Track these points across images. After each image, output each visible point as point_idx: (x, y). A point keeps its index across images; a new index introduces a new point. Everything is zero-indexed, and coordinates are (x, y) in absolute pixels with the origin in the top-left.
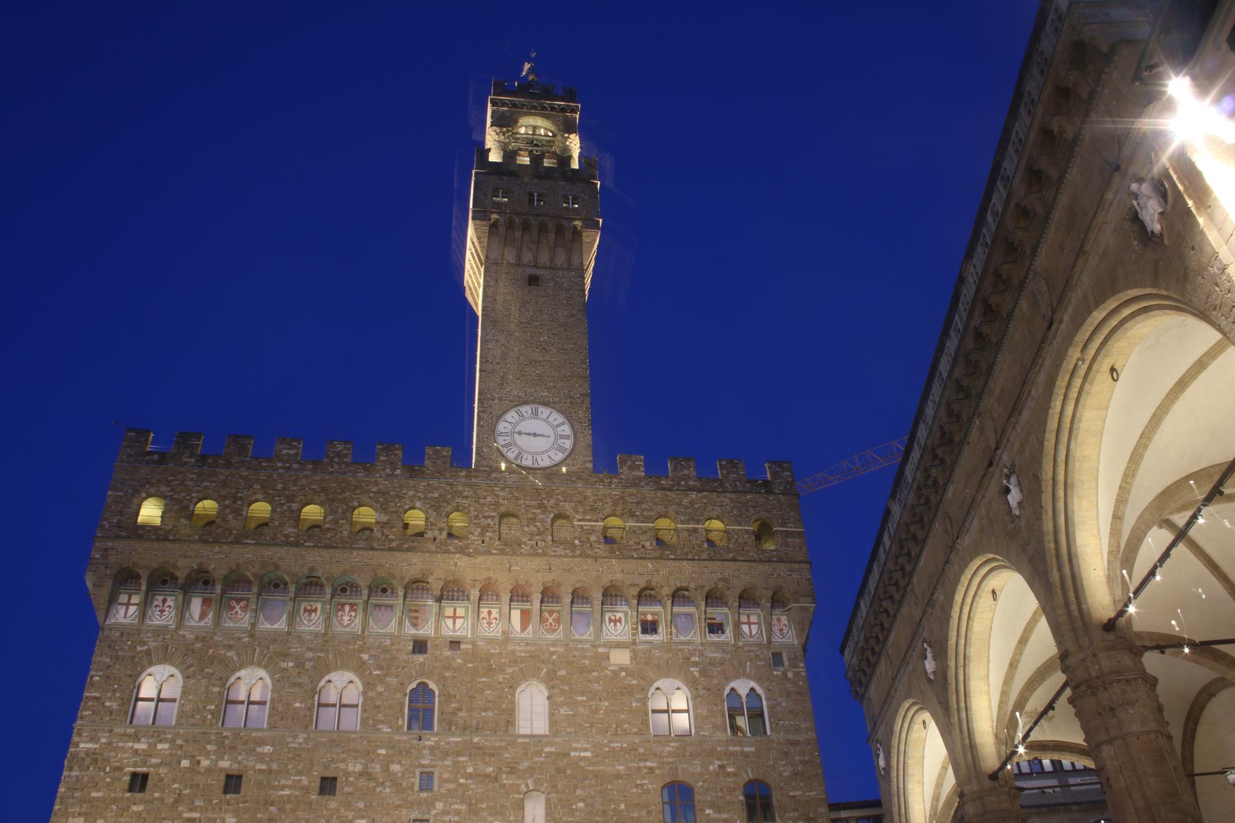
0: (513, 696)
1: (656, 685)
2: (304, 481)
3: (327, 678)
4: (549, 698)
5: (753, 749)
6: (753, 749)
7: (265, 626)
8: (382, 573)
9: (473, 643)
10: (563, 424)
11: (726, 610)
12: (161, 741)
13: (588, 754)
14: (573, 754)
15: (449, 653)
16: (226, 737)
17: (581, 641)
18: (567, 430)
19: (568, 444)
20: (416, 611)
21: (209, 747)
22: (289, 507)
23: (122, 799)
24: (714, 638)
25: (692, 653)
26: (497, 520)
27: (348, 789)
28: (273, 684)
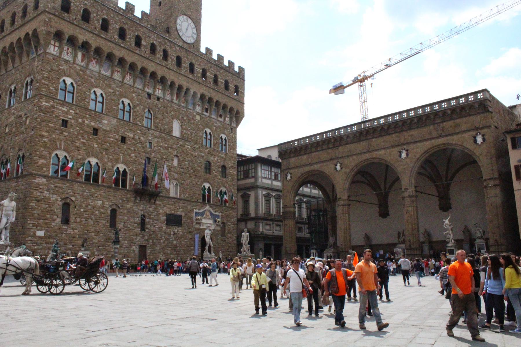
4: (181, 126)
8: (144, 65)
15: (157, 102)
16: (92, 114)
17: (189, 109)
18: (195, 31)
19: (195, 37)
20: (148, 83)
21: (87, 116)
23: (60, 129)
24: (220, 119)
25: (215, 122)
27: (130, 143)
28: (107, 98)
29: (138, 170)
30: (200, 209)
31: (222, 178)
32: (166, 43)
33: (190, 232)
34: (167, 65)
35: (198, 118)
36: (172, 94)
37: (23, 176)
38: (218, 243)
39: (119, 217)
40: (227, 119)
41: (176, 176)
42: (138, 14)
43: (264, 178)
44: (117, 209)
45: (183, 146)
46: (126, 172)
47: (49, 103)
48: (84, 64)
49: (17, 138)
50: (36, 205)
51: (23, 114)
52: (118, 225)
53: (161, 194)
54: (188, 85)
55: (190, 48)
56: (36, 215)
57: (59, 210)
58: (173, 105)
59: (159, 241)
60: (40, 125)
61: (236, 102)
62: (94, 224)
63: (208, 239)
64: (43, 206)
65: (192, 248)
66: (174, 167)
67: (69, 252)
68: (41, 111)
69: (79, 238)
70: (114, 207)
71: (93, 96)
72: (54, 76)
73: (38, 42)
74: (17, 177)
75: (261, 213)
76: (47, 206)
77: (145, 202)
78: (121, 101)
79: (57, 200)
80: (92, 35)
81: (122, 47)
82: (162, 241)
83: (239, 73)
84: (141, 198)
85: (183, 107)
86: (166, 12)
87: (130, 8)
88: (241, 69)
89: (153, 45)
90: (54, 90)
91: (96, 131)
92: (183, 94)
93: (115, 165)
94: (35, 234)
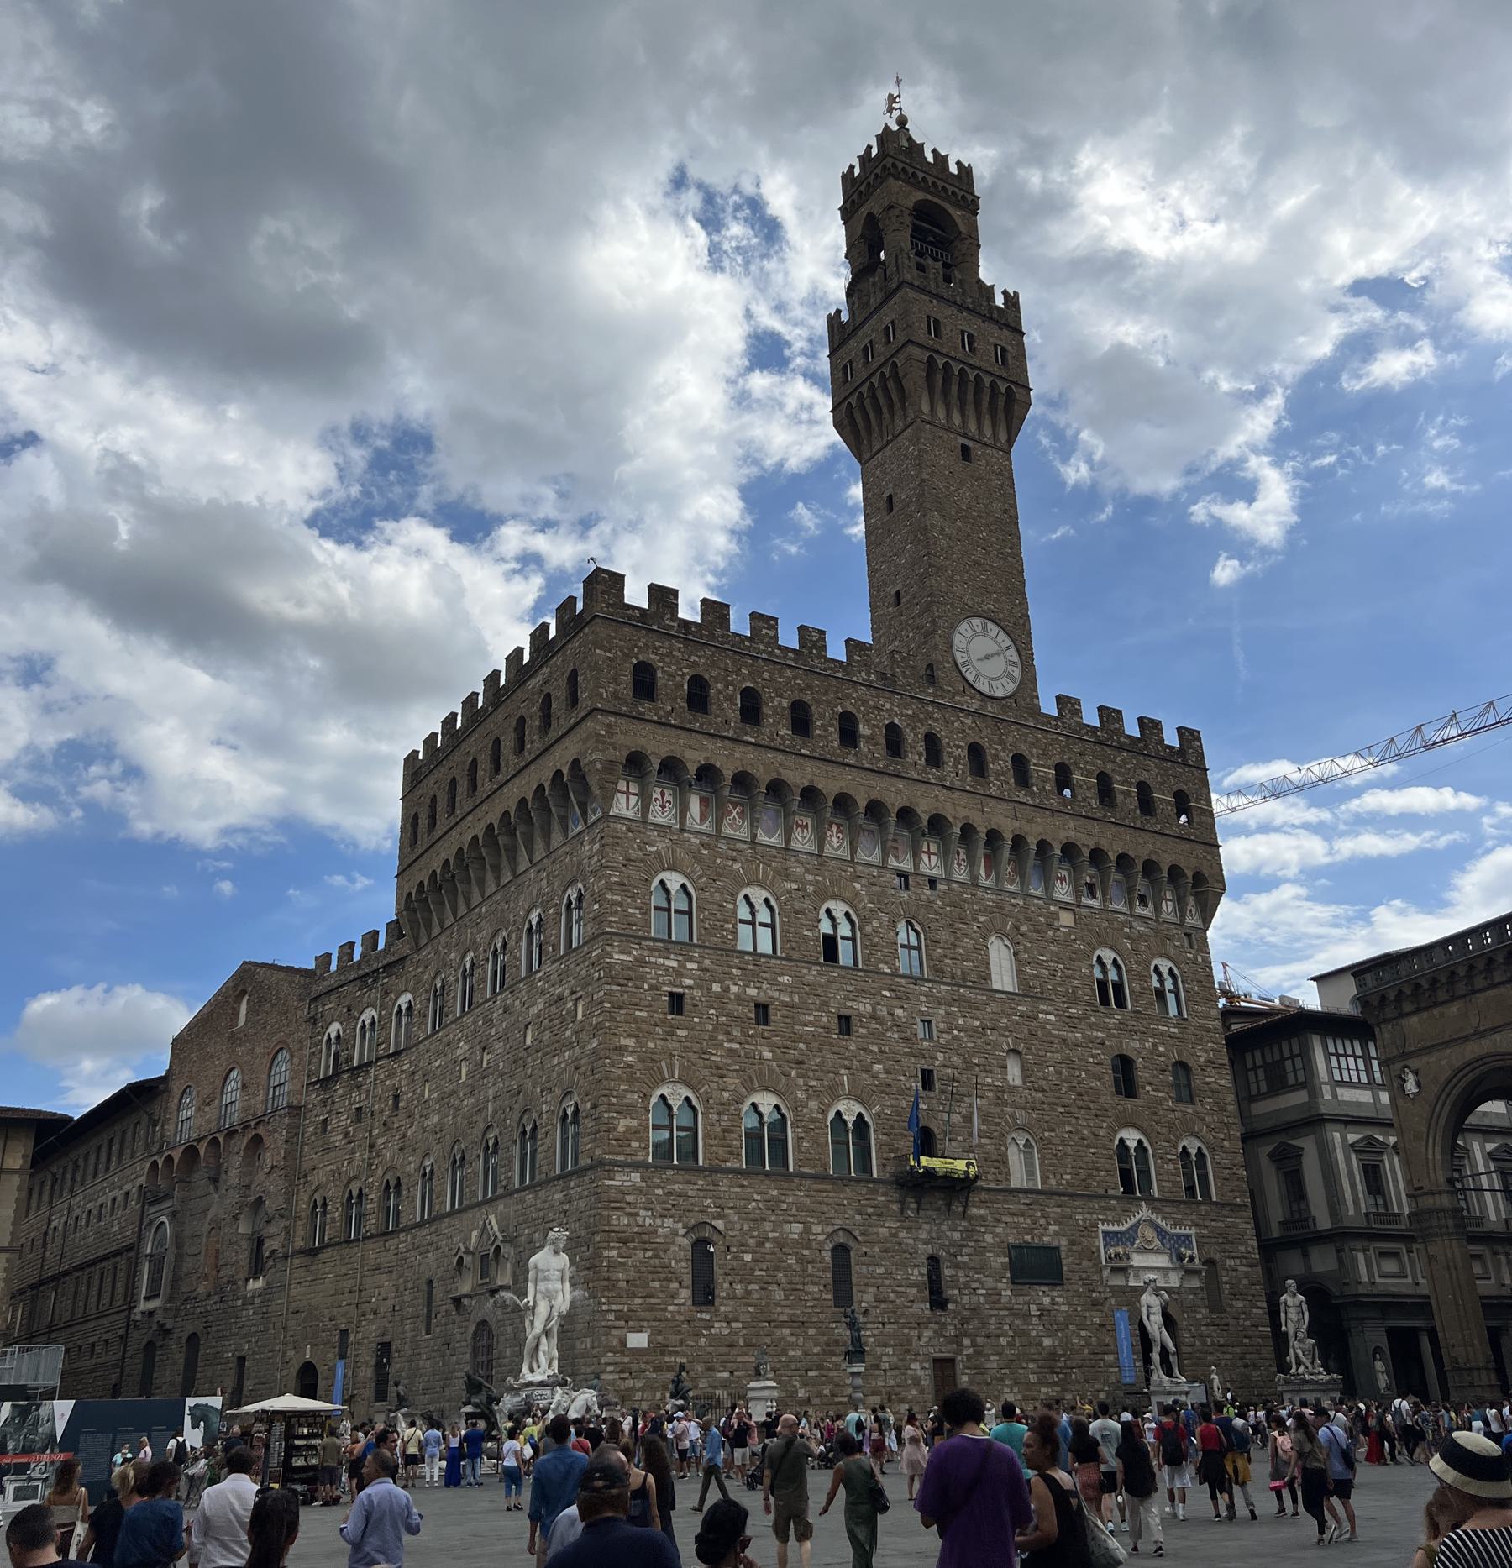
4: (1015, 954)
8: (874, 795)
15: (928, 892)
16: (747, 963)
19: (1017, 672)
20: (895, 841)
24: (1140, 911)
25: (1124, 924)
29: (899, 1114)
30: (1119, 1222)
31: (1181, 1107)
32: (929, 715)
33: (1096, 1304)
34: (942, 778)
35: (1066, 919)
36: (971, 862)
37: (579, 1172)
38: (1202, 1337)
39: (858, 1270)
40: (1167, 906)
41: (1021, 1117)
42: (836, 651)
43: (1341, 1083)
44: (851, 1243)
45: (1030, 1017)
46: (866, 1123)
47: (629, 953)
48: (708, 826)
49: (556, 1061)
50: (620, 1256)
51: (567, 993)
52: (857, 1296)
53: (979, 1183)
54: (1017, 824)
55: (1005, 712)
56: (623, 1284)
57: (684, 1264)
58: (980, 894)
59: (993, 1341)
60: (612, 1019)
61: (1187, 846)
62: (787, 1298)
63: (1155, 1325)
64: (640, 1254)
65: (1110, 1358)
66: (1013, 1090)
67: (721, 1393)
68: (613, 980)
69: (747, 1345)
70: (841, 1238)
71: (743, 912)
72: (636, 875)
73: (586, 789)
74: (565, 1176)
75: (1351, 1212)
76: (649, 1254)
77: (933, 1214)
78: (822, 911)
79: (676, 1234)
82: (1004, 1341)
83: (1181, 751)
84: (918, 1203)
85: (1013, 894)
86: (919, 621)
87: (812, 639)
88: (1189, 737)
89: (892, 729)
91: (762, 1011)
92: (1006, 853)
93: (829, 1106)
94: (623, 1342)
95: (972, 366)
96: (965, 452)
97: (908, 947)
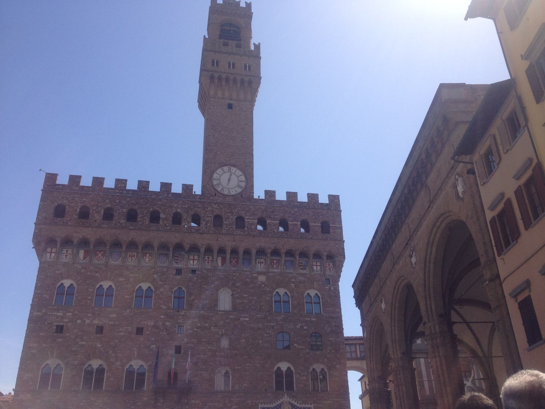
0: (217, 294)
1: (276, 290)
2: (129, 199)
3: (139, 285)
4: (232, 295)
5: (315, 319)
6: (315, 319)
7: (112, 262)
9: (202, 271)
10: (242, 175)
11: (307, 259)
12: (68, 312)
13: (247, 319)
14: (241, 319)
18: (243, 178)
19: (243, 184)
22: (122, 211)
24: (302, 271)
26: (212, 218)
27: (148, 333)
35: (262, 278)
40: (317, 268)
54: (234, 243)
80: (90, 229)
81: (131, 229)
90: (48, 297)
92: (228, 256)
95: (232, 74)
96: (230, 106)
97: (179, 298)
